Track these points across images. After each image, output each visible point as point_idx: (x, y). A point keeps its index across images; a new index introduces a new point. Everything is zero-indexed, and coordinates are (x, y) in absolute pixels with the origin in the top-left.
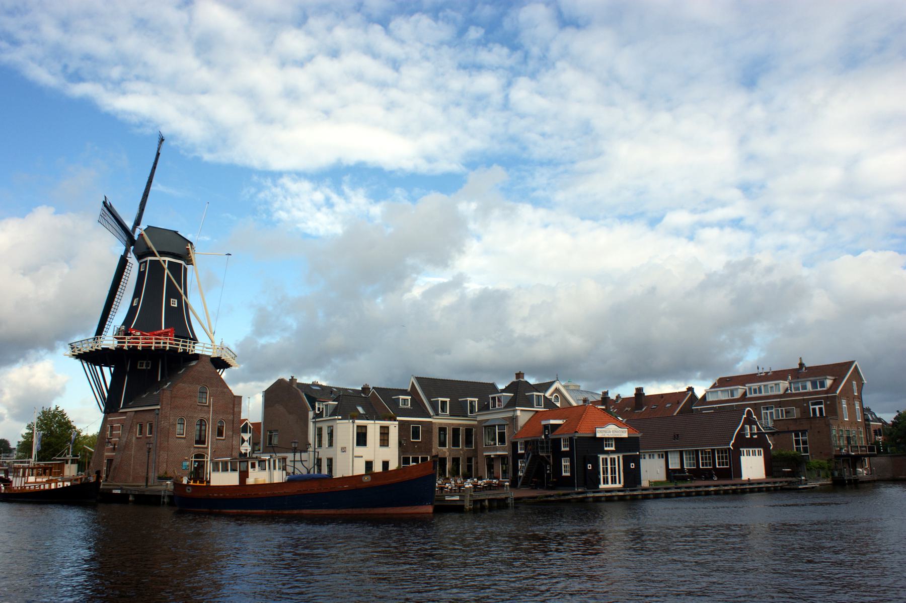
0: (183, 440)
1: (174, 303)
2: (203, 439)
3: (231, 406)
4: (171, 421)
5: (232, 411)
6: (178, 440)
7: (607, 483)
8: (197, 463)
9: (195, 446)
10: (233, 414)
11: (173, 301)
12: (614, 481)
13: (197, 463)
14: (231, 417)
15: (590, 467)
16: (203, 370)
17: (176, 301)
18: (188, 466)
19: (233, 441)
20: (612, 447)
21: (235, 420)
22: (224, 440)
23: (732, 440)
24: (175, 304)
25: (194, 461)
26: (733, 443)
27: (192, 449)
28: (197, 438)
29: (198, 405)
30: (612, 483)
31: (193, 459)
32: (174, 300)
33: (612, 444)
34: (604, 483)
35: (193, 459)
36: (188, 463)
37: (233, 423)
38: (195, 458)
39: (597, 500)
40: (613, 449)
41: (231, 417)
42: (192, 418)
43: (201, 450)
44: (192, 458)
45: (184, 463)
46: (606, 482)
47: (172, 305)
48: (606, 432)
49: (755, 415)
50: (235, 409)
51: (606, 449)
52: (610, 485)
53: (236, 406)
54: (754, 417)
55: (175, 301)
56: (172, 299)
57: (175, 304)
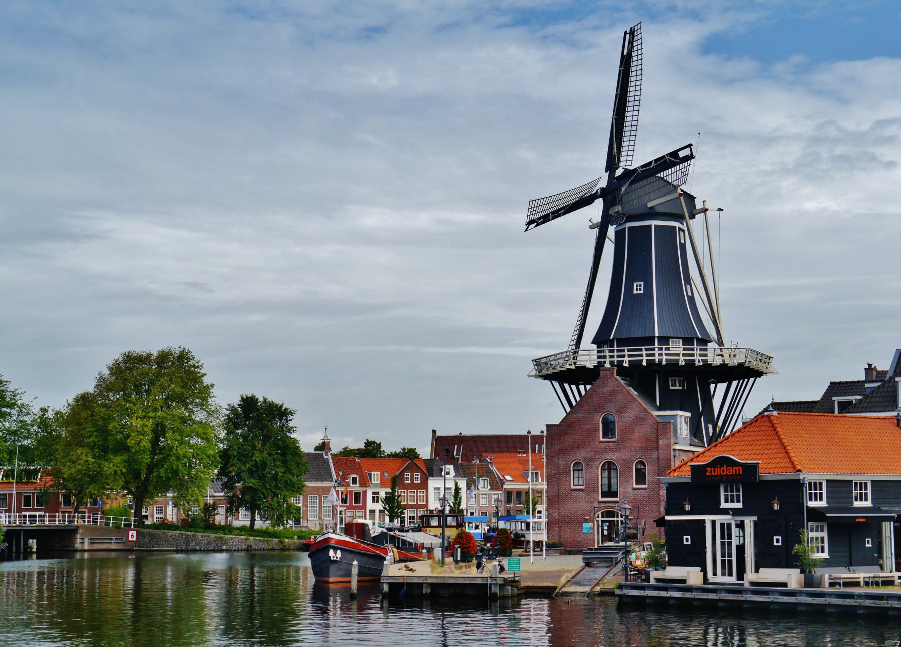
0: (581, 493)
1: (638, 288)
2: (614, 488)
3: (654, 436)
4: (561, 467)
5: (655, 445)
6: (574, 494)
8: (607, 524)
9: (601, 500)
10: (657, 449)
11: (637, 286)
13: (607, 524)
14: (654, 454)
17: (642, 283)
18: (590, 528)
19: (659, 491)
20: (738, 501)
21: (661, 457)
22: (645, 489)
24: (640, 290)
25: (603, 522)
27: (596, 505)
28: (606, 489)
29: (600, 442)
31: (600, 519)
32: (639, 283)
33: (738, 496)
34: (723, 575)
35: (600, 519)
36: (590, 525)
37: (658, 463)
38: (602, 517)
40: (740, 505)
41: (654, 454)
42: (592, 460)
43: (610, 505)
44: (598, 517)
45: (584, 524)
50: (660, 441)
51: (724, 505)
53: (660, 437)
55: (640, 286)
56: (635, 284)
57: (640, 290)
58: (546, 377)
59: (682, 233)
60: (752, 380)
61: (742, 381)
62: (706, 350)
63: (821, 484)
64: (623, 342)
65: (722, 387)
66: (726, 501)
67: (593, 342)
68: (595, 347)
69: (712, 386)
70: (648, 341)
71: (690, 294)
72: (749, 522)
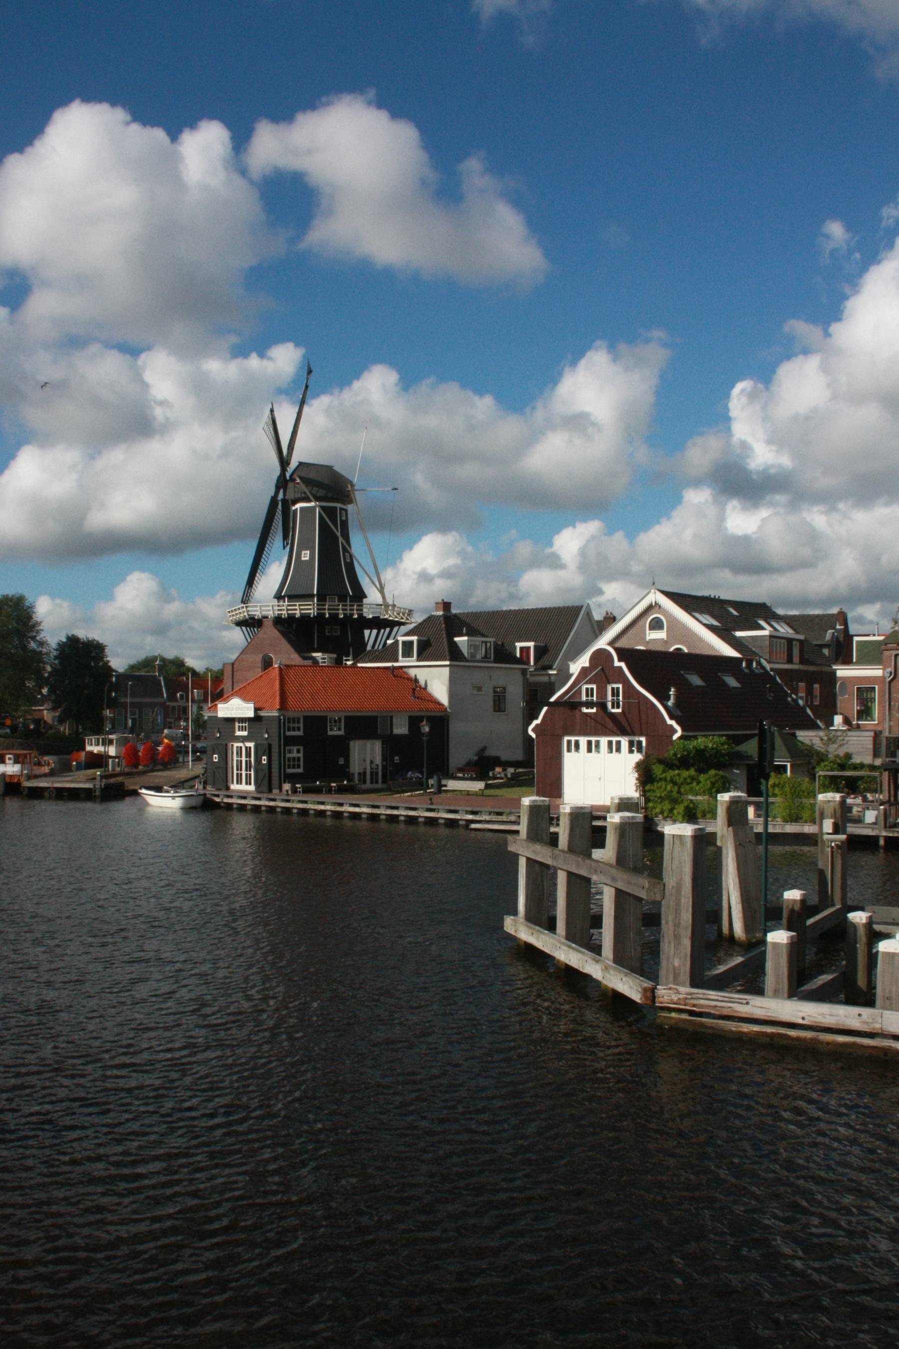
1: (306, 556)
7: (241, 783)
12: (248, 783)
15: (216, 758)
16: (266, 636)
23: (537, 718)
26: (537, 725)
30: (246, 784)
32: (306, 552)
39: (229, 806)
40: (245, 733)
46: (239, 782)
47: (303, 559)
48: (227, 709)
49: (620, 660)
52: (243, 787)
54: (617, 663)
58: (239, 624)
59: (343, 512)
60: (396, 629)
61: (388, 630)
62: (362, 606)
63: (299, 719)
64: (292, 597)
65: (375, 632)
66: (239, 730)
67: (275, 597)
68: (276, 600)
69: (367, 632)
70: (309, 596)
71: (348, 560)
72: (251, 745)
